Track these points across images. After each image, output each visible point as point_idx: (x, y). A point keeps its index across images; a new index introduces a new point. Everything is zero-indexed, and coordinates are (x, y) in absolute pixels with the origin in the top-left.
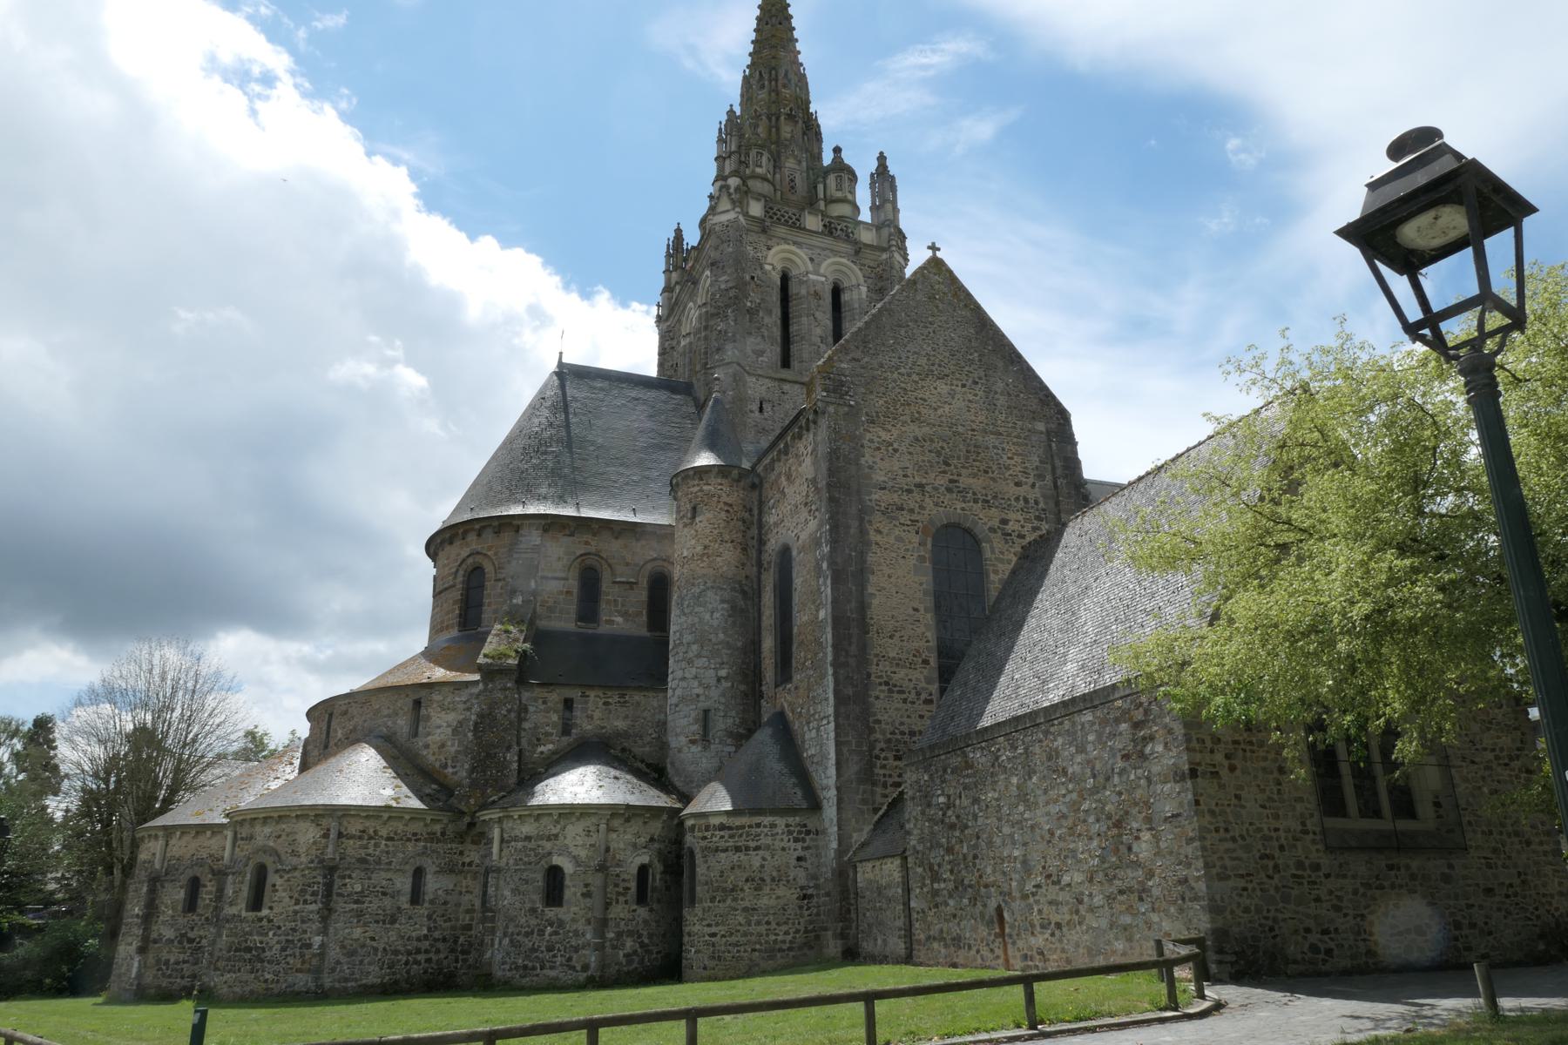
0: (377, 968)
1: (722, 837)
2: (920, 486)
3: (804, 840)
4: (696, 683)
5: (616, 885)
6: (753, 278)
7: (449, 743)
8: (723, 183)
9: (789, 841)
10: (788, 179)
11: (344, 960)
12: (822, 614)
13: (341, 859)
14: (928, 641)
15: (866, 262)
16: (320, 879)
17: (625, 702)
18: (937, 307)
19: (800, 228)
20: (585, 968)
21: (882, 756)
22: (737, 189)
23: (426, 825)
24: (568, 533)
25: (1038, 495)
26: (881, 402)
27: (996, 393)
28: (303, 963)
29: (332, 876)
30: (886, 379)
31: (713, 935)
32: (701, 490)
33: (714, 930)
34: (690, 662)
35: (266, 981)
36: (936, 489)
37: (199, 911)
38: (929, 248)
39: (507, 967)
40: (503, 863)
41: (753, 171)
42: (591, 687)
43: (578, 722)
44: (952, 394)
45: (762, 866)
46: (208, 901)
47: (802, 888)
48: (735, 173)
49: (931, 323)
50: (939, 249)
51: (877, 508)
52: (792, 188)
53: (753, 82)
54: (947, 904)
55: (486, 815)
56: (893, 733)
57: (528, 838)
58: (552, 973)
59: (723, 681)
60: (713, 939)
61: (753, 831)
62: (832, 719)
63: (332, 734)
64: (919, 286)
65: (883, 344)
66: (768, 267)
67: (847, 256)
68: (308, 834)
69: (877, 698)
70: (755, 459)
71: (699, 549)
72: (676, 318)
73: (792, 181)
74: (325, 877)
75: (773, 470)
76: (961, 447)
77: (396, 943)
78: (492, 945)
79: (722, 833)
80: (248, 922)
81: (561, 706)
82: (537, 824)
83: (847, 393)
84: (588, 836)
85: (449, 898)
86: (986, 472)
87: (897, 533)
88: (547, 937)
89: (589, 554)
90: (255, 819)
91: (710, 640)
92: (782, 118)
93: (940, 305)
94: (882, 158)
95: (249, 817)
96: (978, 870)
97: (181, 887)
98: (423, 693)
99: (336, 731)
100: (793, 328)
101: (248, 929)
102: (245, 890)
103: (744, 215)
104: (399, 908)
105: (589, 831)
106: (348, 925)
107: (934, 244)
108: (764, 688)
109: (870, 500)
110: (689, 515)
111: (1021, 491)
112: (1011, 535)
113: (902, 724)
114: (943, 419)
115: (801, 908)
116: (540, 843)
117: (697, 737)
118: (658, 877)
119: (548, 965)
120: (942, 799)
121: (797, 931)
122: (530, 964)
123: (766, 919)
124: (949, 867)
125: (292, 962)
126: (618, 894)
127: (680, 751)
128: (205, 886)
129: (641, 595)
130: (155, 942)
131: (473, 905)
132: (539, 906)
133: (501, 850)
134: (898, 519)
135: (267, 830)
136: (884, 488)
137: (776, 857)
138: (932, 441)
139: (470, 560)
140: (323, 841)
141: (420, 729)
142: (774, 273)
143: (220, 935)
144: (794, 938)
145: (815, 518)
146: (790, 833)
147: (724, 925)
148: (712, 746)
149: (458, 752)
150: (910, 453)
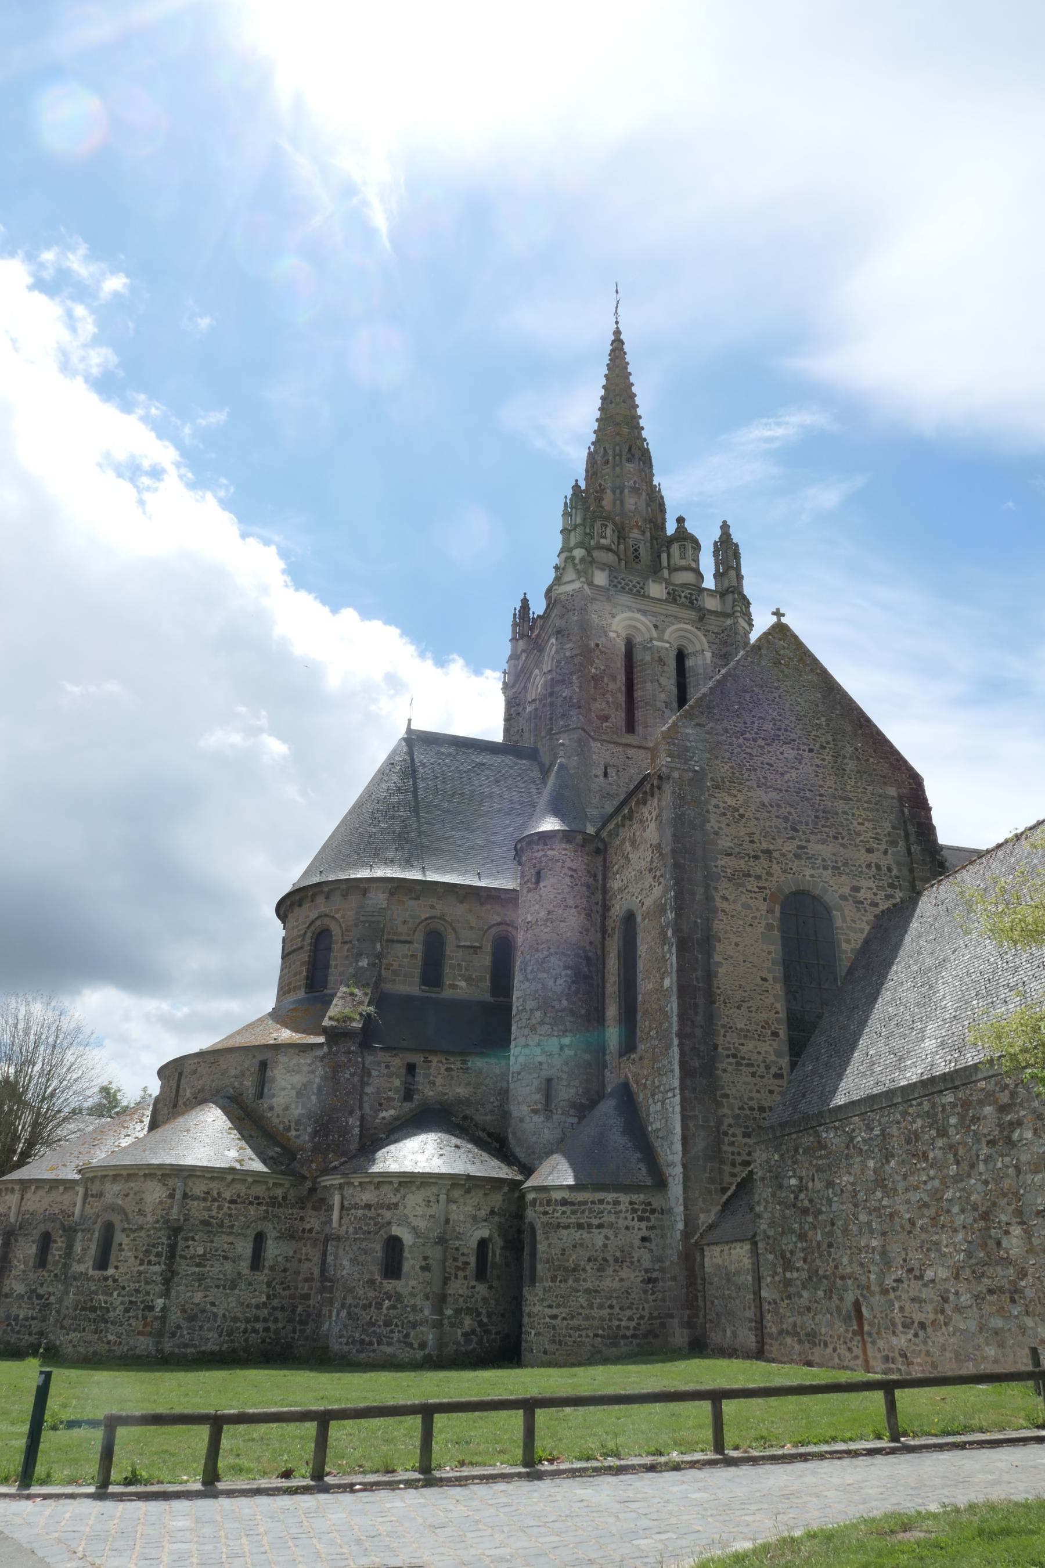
0: (216, 1335)
1: (564, 1213)
2: (768, 852)
3: (648, 1219)
4: (538, 1051)
5: (455, 1259)
6: (597, 645)
7: (293, 1106)
8: (569, 554)
9: (633, 1219)
10: (632, 549)
11: (184, 1324)
12: (667, 982)
13: (185, 1220)
14: (777, 1013)
15: (711, 628)
16: (164, 1240)
17: (468, 1069)
18: (782, 672)
19: (644, 596)
20: (423, 1345)
21: (730, 1132)
22: (582, 560)
23: (268, 1189)
24: (413, 896)
25: (892, 862)
26: (726, 767)
27: (845, 757)
28: (145, 1325)
29: (176, 1237)
30: (731, 744)
31: (554, 1317)
32: (545, 855)
34: (533, 1029)
35: (109, 1342)
36: (783, 855)
37: (49, 1267)
38: (774, 614)
39: (344, 1340)
40: (342, 1232)
41: (598, 542)
42: (434, 1052)
43: (420, 1088)
44: (799, 759)
45: (605, 1246)
46: (57, 1258)
47: (647, 1271)
48: (580, 545)
49: (776, 688)
50: (783, 615)
51: (723, 874)
52: (637, 557)
53: (598, 458)
54: (801, 1296)
55: (328, 1181)
56: (742, 1108)
57: (368, 1206)
58: (389, 1350)
59: (566, 1049)
60: (554, 1322)
61: (597, 1207)
62: (677, 1091)
63: (181, 1093)
64: (764, 652)
65: (728, 710)
66: (612, 635)
67: (692, 622)
68: (155, 1193)
69: (725, 1071)
70: (599, 825)
71: (543, 914)
72: (522, 685)
73: (636, 550)
74: (169, 1238)
75: (617, 835)
76: (810, 812)
77: (236, 1310)
78: (330, 1317)
79: (564, 1208)
80: (94, 1280)
81: (403, 1071)
82: (377, 1192)
83: (691, 758)
84: (428, 1206)
85: (288, 1265)
86: (836, 838)
87: (744, 900)
88: (384, 1311)
89: (434, 917)
90: (106, 1176)
91: (553, 1007)
92: (626, 491)
93: (786, 670)
94: (725, 527)
95: (99, 1174)
96: (834, 1260)
97: (33, 1242)
99: (185, 1090)
100: (638, 694)
101: (94, 1288)
103: (589, 585)
104: (239, 1273)
105: (429, 1201)
106: (190, 1288)
107: (778, 609)
108: (608, 1058)
109: (716, 867)
110: (533, 880)
111: (873, 858)
112: (862, 903)
113: (751, 1099)
114: (790, 784)
115: (645, 1292)
116: (380, 1211)
117: (539, 1107)
118: (498, 1252)
119: (385, 1340)
120: (793, 1181)
121: (642, 1317)
122: (367, 1339)
123: (609, 1302)
124: (802, 1255)
125: (134, 1324)
126: (458, 1268)
127: (522, 1120)
128: (55, 1242)
129: (485, 959)
130: (7, 1296)
131: (312, 1274)
132: (378, 1278)
133: (341, 1218)
134: (744, 886)
135: (117, 1188)
136: (731, 854)
137: (620, 1236)
138: (779, 806)
139: (318, 923)
140: (169, 1201)
141: (266, 1090)
142: (618, 640)
143: (67, 1293)
144: (639, 1324)
145: (660, 884)
146: (634, 1211)
147: (565, 1307)
148: (555, 1117)
149: (301, 1115)
150: (757, 819)
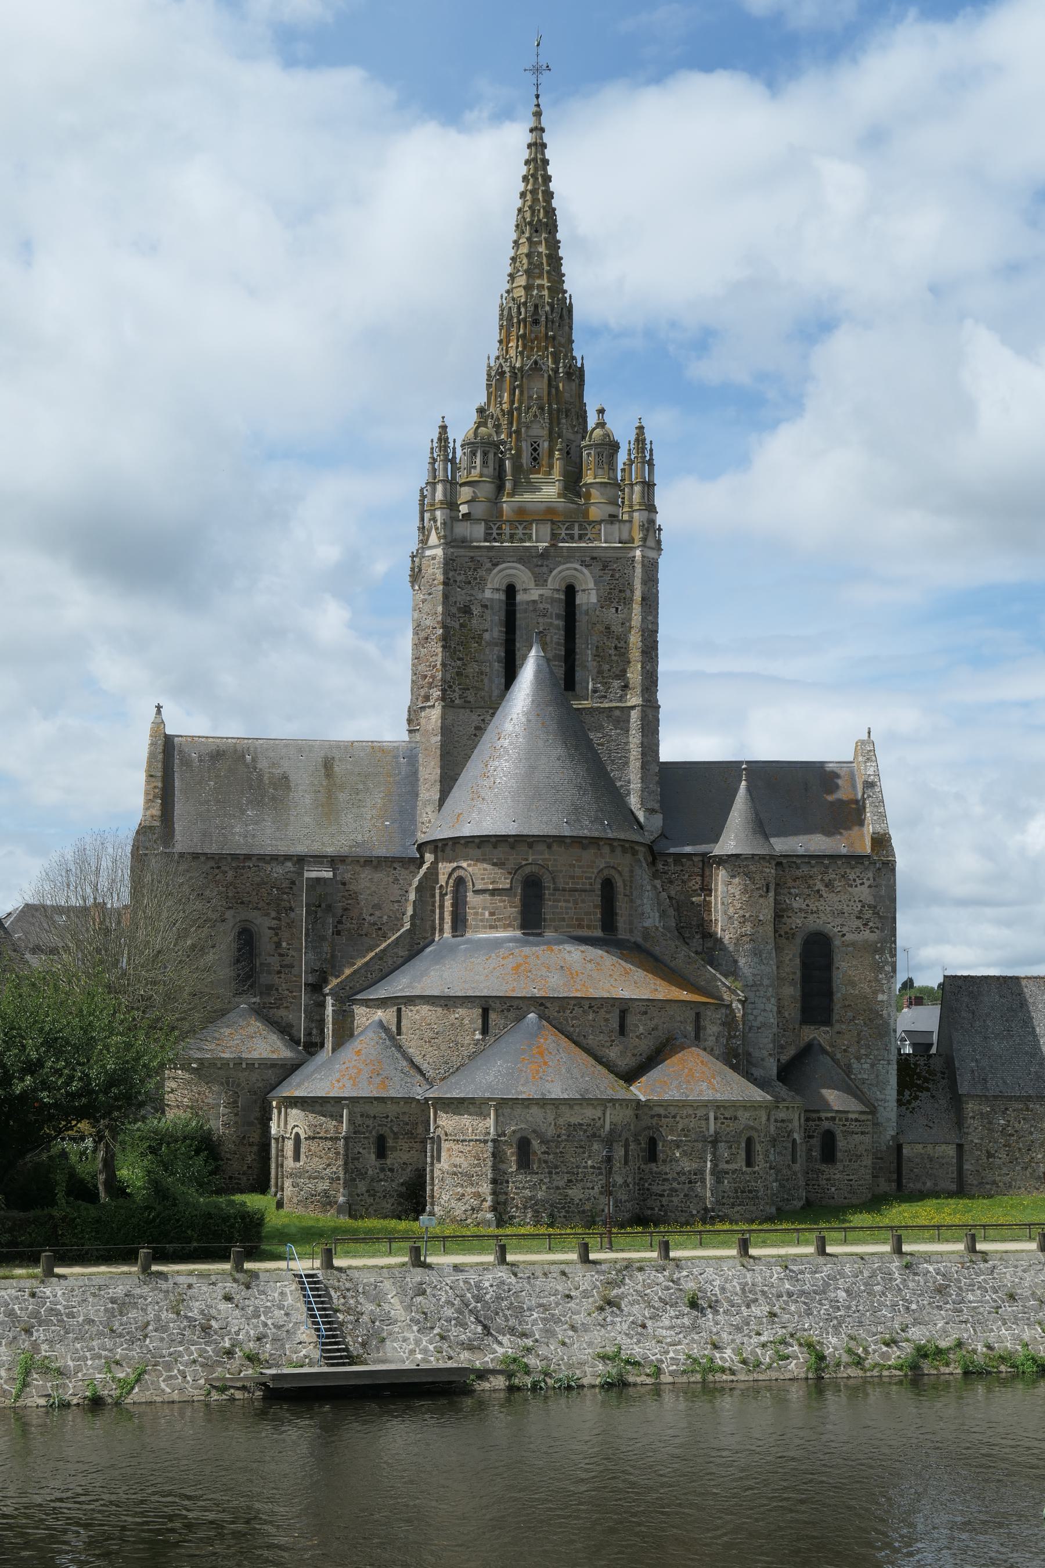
31: (851, 1180)
33: (851, 1177)
127: (763, 1060)
145: (872, 932)
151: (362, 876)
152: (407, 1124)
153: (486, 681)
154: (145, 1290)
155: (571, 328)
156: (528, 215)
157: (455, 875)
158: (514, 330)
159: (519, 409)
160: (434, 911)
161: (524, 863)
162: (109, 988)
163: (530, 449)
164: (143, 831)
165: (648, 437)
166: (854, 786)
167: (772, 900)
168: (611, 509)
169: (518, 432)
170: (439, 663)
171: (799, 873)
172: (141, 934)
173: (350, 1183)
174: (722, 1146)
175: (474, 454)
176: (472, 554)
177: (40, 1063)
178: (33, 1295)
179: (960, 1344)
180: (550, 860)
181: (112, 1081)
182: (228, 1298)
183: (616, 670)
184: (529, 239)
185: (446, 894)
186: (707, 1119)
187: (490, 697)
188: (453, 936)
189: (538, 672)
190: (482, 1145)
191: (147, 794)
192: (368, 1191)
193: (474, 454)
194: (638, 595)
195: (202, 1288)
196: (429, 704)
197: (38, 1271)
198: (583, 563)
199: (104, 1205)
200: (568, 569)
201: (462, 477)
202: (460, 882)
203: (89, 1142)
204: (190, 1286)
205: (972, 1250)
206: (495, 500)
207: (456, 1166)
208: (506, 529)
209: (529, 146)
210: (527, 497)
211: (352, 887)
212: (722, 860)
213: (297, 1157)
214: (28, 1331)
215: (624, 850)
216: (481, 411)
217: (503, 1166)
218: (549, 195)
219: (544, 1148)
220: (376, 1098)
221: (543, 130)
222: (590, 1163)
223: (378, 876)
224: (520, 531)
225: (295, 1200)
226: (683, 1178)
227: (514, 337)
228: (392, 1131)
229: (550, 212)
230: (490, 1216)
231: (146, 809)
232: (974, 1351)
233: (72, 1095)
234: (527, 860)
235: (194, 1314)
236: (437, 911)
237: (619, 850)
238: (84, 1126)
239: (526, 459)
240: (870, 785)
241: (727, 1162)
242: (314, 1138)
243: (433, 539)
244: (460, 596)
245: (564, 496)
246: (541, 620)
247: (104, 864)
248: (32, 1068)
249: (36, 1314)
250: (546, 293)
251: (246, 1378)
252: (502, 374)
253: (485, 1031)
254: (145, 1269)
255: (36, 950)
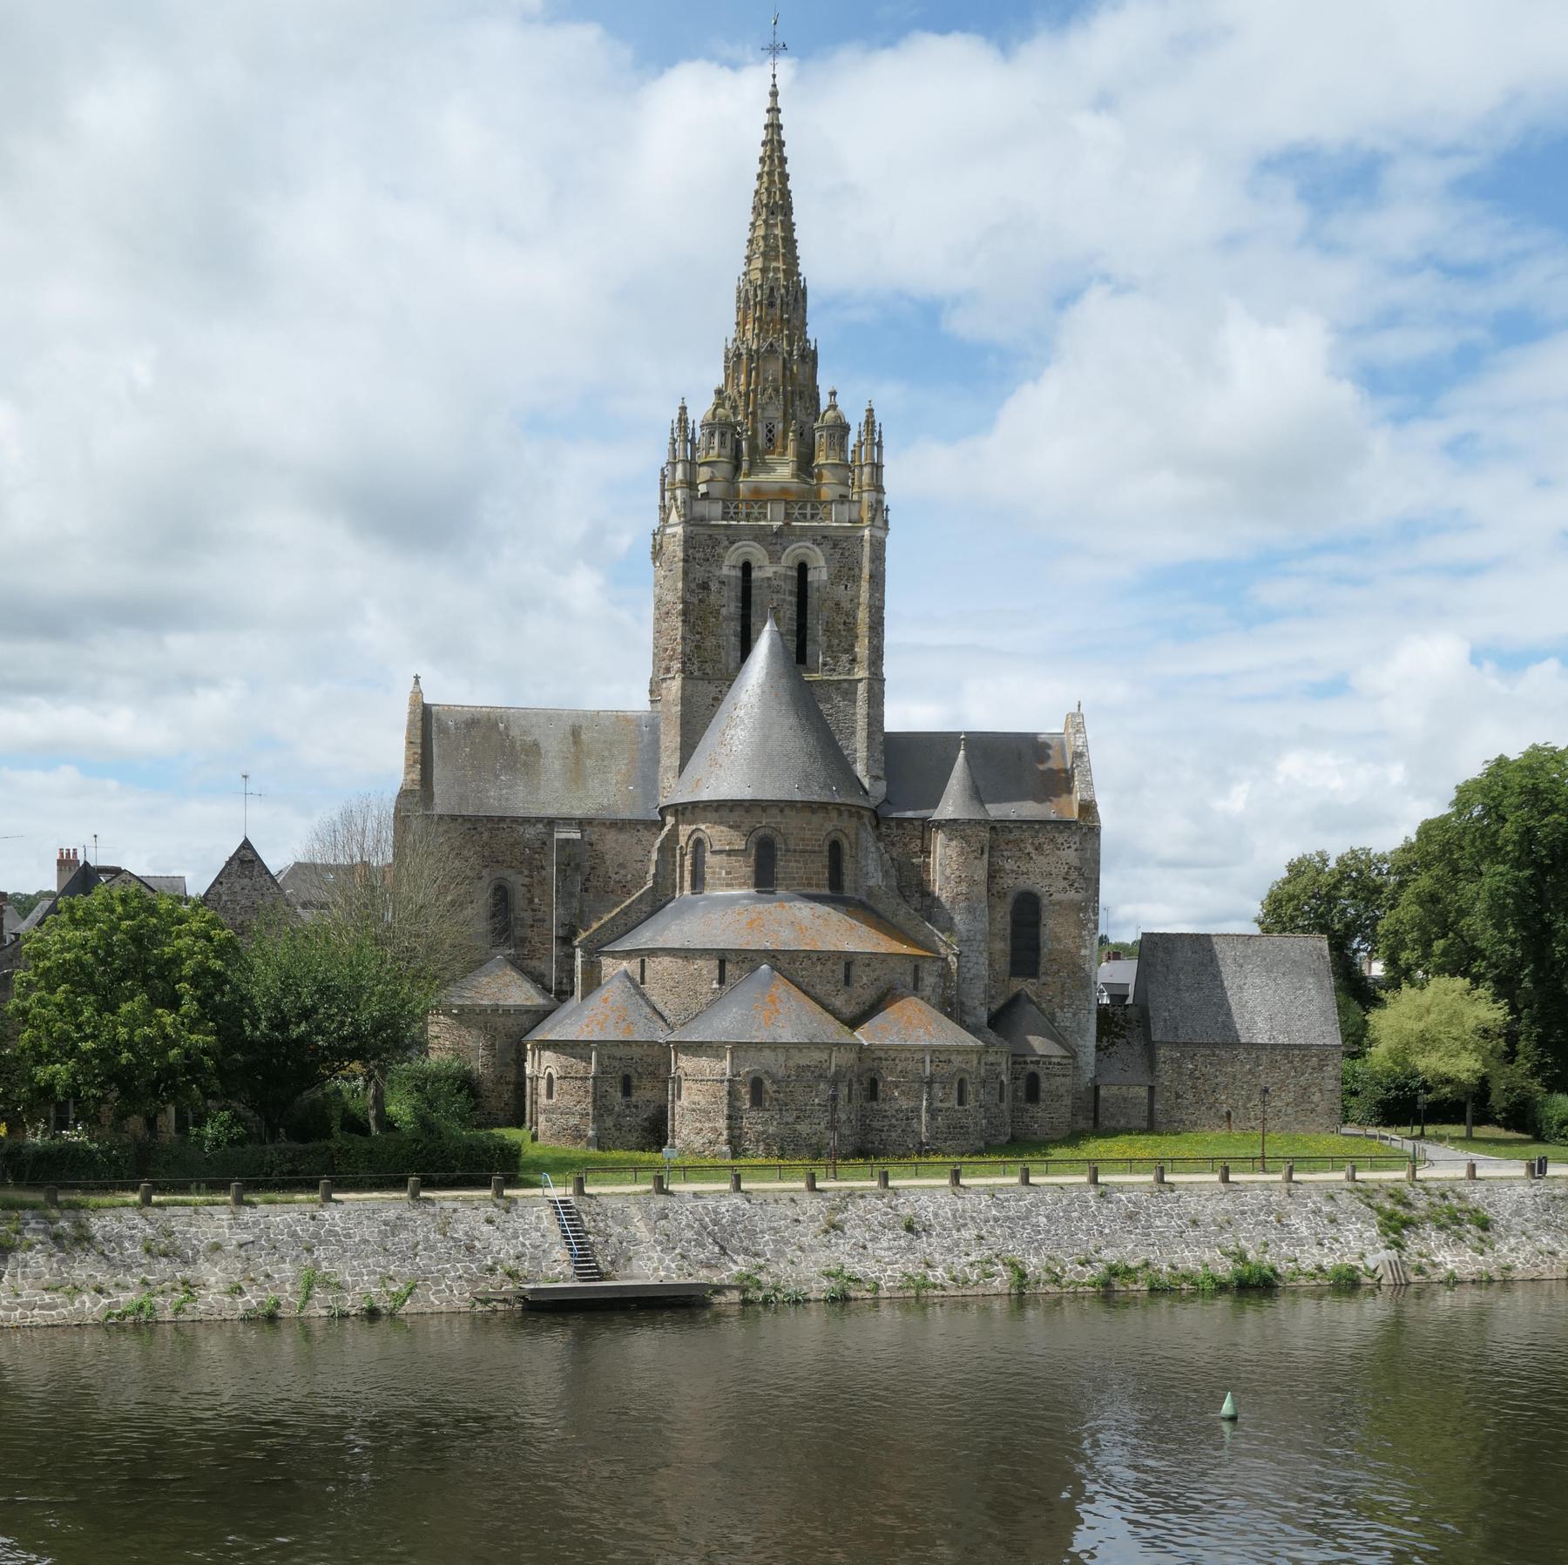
98: (920, 962)
102: (955, 1094)
120: (1190, 1066)
127: (975, 1008)
151: (608, 837)
152: (650, 1065)
153: (723, 654)
154: (415, 1213)
155: (805, 311)
156: (764, 197)
157: (694, 837)
158: (751, 312)
159: (755, 391)
160: (675, 871)
161: (758, 825)
162: (377, 940)
163: (765, 430)
164: (404, 794)
165: (878, 418)
166: (1064, 756)
167: (986, 862)
168: (841, 490)
169: (754, 413)
170: (679, 637)
171: (1011, 837)
172: (404, 889)
173: (598, 1118)
174: (936, 1086)
175: (712, 435)
176: (710, 533)
177: (314, 1009)
178: (313, 1218)
179: (1147, 1264)
180: (782, 823)
181: (379, 1026)
182: (490, 1221)
183: (845, 645)
184: (765, 221)
185: (686, 854)
186: (924, 1062)
187: (727, 669)
188: (693, 894)
189: (772, 645)
190: (719, 1084)
191: (407, 759)
192: (614, 1126)
193: (712, 435)
194: (866, 573)
195: (466, 1212)
196: (669, 676)
197: (317, 1196)
198: (815, 541)
199: (376, 1138)
200: (800, 547)
201: (701, 457)
202: (699, 843)
203: (360, 1082)
204: (455, 1211)
205: (1161, 1181)
206: (732, 480)
207: (694, 1103)
208: (743, 508)
209: (766, 127)
210: (762, 477)
211: (598, 847)
212: (940, 825)
213: (550, 1095)
214: (309, 1250)
215: (851, 815)
216: (719, 392)
217: (738, 1104)
218: (785, 177)
219: (775, 1087)
220: (622, 1042)
221: (779, 111)
222: (817, 1101)
223: (623, 837)
224: (756, 511)
225: (548, 1134)
226: (901, 1115)
227: (750, 320)
228: (637, 1071)
229: (786, 194)
230: (725, 1148)
231: (407, 774)
232: (1160, 1271)
233: (345, 1039)
234: (761, 823)
235: (460, 1235)
236: (678, 870)
237: (846, 815)
238: (356, 1066)
239: (761, 441)
240: (1079, 755)
241: (941, 1101)
242: (565, 1078)
243: (674, 518)
244: (699, 573)
245: (798, 477)
246: (775, 596)
247: (369, 824)
248: (306, 1014)
249: (316, 1235)
250: (781, 275)
251: (507, 1292)
252: (740, 355)
253: (721, 981)
254: (414, 1195)
255: (305, 906)
